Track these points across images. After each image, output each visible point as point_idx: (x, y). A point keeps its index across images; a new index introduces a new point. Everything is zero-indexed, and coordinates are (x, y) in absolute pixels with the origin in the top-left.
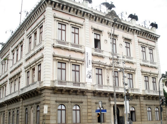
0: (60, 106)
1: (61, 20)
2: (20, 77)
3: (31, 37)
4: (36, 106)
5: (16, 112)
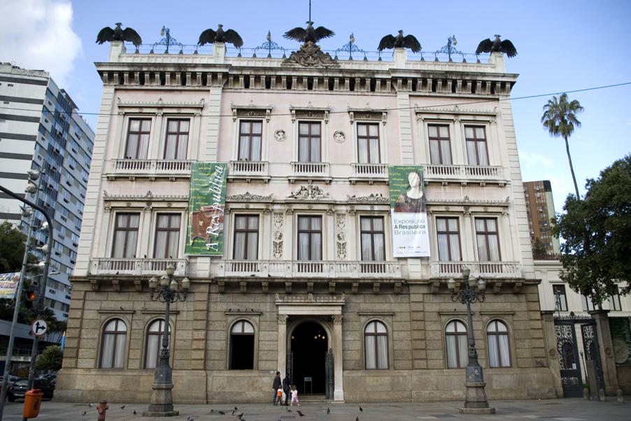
0: (494, 324)
1: (137, 110)
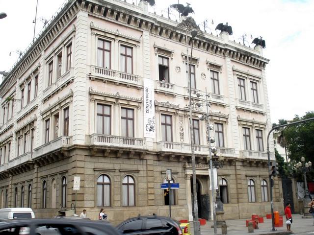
0: (102, 177)
1: (103, 34)
2: (33, 130)
3: (52, 62)
4: (60, 177)
5: (26, 188)
